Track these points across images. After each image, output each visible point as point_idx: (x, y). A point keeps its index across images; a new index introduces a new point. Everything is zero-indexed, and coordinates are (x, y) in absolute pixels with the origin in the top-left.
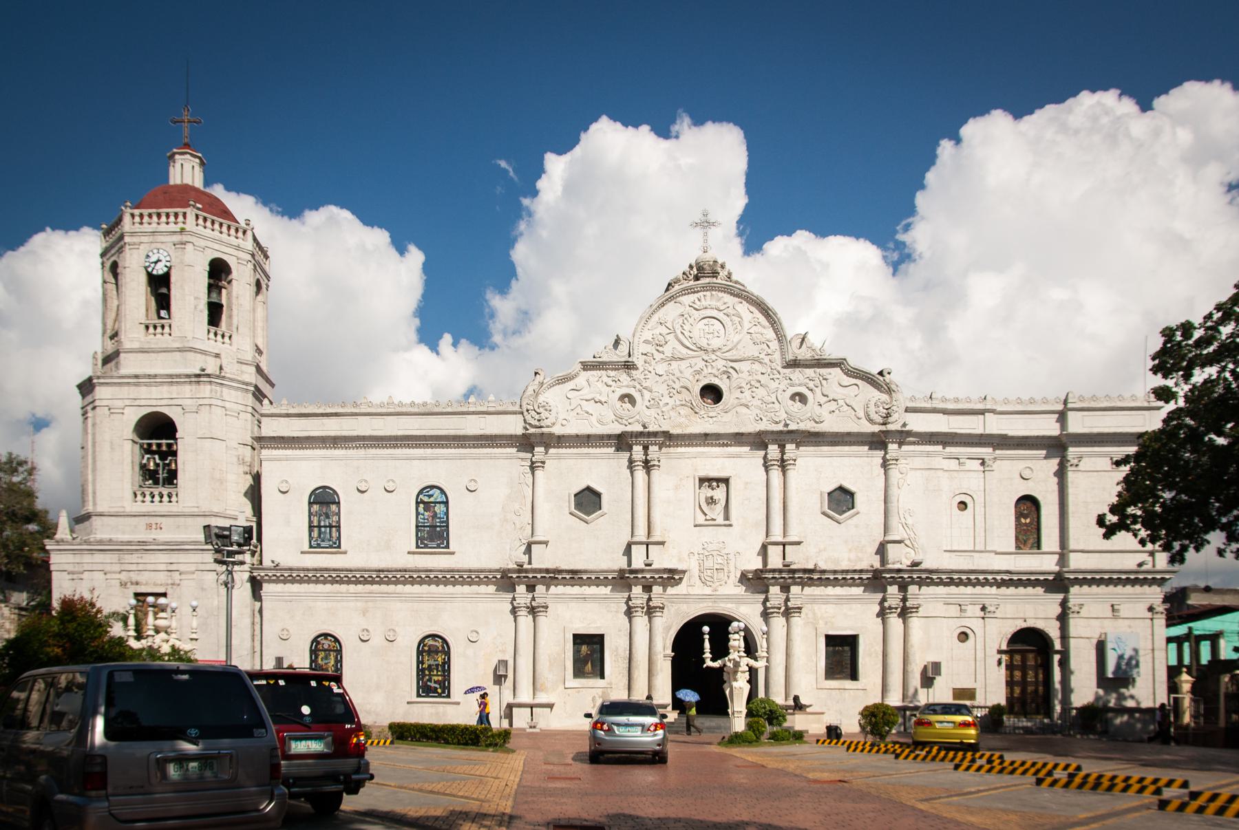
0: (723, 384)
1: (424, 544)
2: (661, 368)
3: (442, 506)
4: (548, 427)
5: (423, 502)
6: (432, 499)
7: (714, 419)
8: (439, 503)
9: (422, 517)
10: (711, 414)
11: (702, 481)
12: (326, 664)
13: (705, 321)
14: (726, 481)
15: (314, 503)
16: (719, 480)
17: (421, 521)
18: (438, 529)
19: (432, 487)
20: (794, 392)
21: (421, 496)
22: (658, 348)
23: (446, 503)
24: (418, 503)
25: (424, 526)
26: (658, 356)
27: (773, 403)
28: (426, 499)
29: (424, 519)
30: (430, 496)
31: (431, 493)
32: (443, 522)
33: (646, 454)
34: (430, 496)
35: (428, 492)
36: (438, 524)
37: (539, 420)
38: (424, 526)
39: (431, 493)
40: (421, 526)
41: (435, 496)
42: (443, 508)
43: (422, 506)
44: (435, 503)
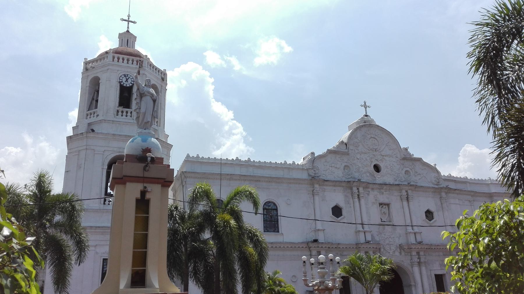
1: (267, 230)
2: (358, 156)
3: (275, 211)
4: (318, 177)
5: (266, 209)
6: (270, 208)
8: (274, 209)
9: (266, 216)
11: (381, 204)
13: (372, 139)
14: (388, 205)
16: (385, 204)
17: (265, 218)
18: (273, 222)
19: (269, 202)
20: (407, 170)
21: (265, 206)
22: (357, 148)
23: (277, 210)
24: (263, 209)
25: (267, 221)
26: (357, 151)
27: (400, 174)
28: (267, 208)
29: (267, 217)
30: (269, 206)
31: (269, 204)
32: (275, 219)
33: (358, 192)
34: (269, 206)
35: (268, 204)
36: (273, 220)
37: (315, 174)
38: (267, 221)
39: (269, 204)
40: (266, 221)
41: (271, 206)
42: (275, 212)
43: (265, 211)
44: (271, 209)
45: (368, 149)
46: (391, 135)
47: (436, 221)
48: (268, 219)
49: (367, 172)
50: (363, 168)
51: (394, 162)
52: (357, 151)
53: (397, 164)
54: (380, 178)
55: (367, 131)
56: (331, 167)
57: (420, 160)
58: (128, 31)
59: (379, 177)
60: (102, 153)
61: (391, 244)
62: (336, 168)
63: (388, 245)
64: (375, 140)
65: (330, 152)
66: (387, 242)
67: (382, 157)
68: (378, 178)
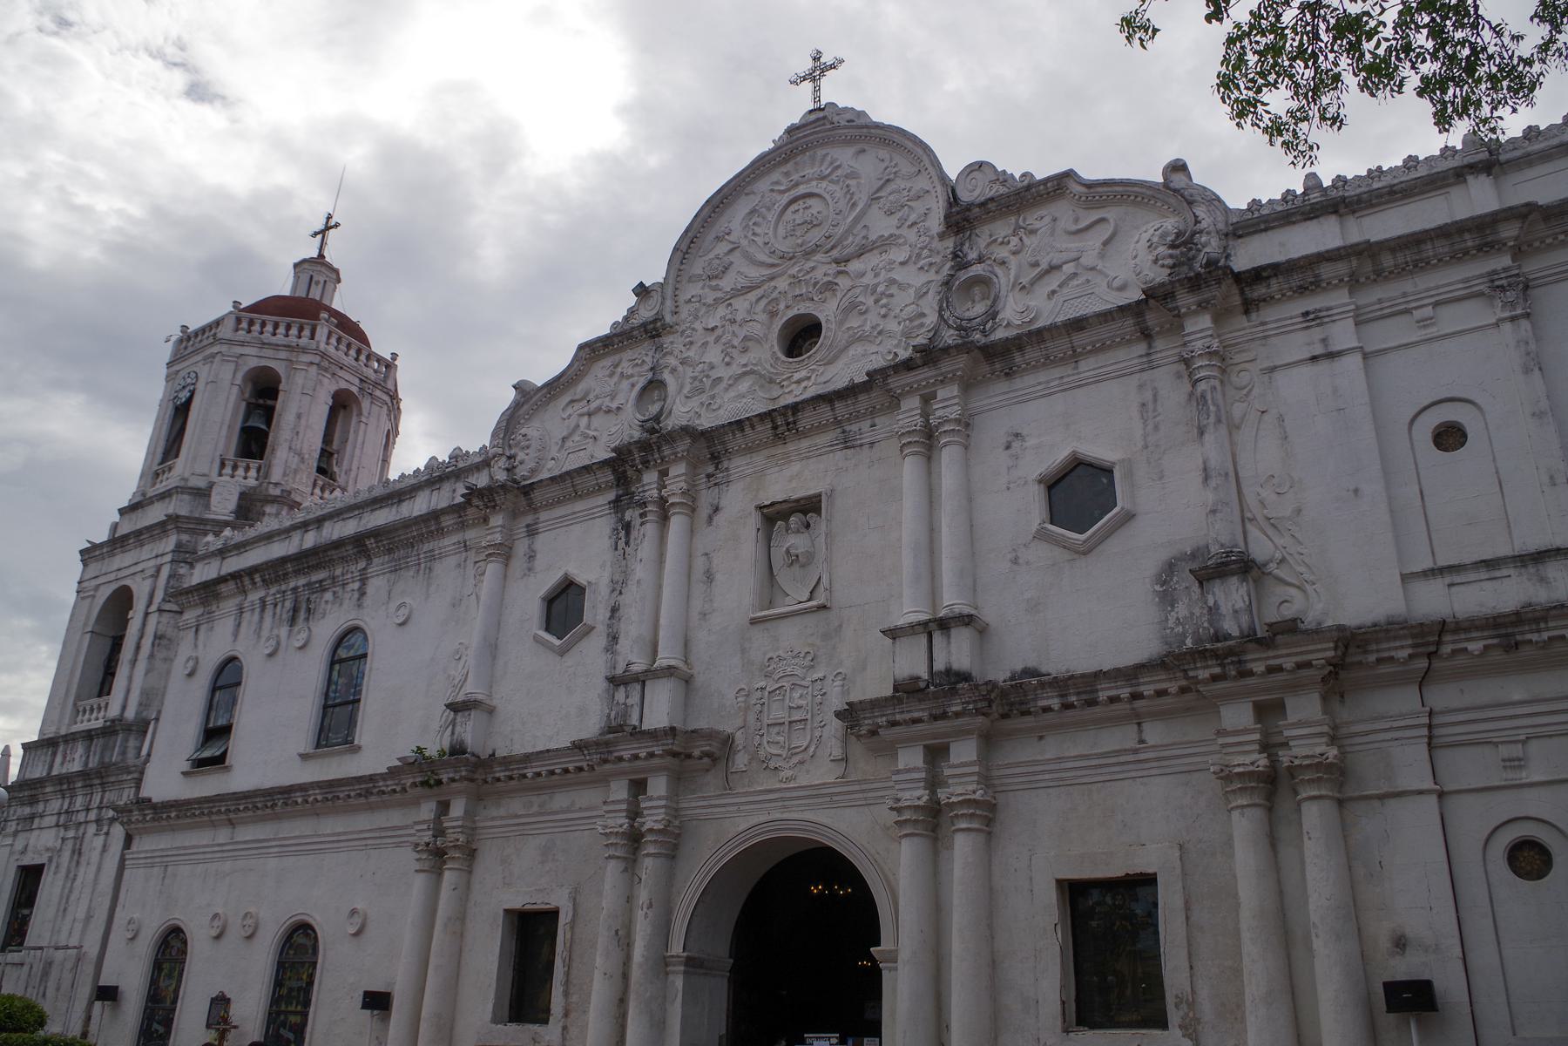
0: (826, 312)
5: (341, 661)
6: (352, 653)
7: (804, 384)
10: (797, 376)
12: (167, 987)
15: (220, 688)
22: (714, 283)
30: (350, 647)
31: (352, 641)
41: (356, 647)
45: (770, 261)
46: (897, 138)
47: (1129, 517)
48: (339, 697)
49: (745, 374)
50: (728, 364)
51: (902, 264)
52: (710, 297)
53: (922, 268)
54: (809, 378)
55: (777, 183)
56: (590, 415)
57: (1061, 184)
58: (321, 256)
59: (803, 373)
60: (91, 593)
61: (790, 722)
62: (609, 411)
63: (776, 729)
64: (810, 202)
65: (592, 351)
66: (777, 712)
67: (834, 268)
68: (798, 382)
